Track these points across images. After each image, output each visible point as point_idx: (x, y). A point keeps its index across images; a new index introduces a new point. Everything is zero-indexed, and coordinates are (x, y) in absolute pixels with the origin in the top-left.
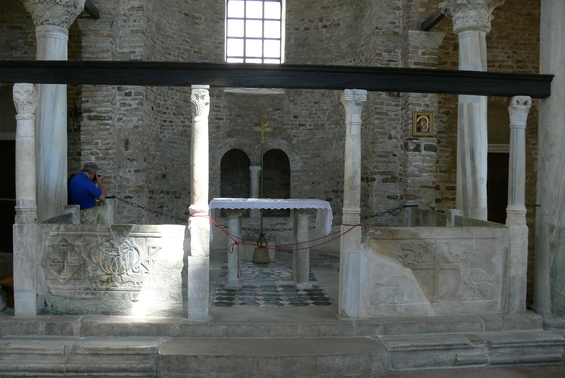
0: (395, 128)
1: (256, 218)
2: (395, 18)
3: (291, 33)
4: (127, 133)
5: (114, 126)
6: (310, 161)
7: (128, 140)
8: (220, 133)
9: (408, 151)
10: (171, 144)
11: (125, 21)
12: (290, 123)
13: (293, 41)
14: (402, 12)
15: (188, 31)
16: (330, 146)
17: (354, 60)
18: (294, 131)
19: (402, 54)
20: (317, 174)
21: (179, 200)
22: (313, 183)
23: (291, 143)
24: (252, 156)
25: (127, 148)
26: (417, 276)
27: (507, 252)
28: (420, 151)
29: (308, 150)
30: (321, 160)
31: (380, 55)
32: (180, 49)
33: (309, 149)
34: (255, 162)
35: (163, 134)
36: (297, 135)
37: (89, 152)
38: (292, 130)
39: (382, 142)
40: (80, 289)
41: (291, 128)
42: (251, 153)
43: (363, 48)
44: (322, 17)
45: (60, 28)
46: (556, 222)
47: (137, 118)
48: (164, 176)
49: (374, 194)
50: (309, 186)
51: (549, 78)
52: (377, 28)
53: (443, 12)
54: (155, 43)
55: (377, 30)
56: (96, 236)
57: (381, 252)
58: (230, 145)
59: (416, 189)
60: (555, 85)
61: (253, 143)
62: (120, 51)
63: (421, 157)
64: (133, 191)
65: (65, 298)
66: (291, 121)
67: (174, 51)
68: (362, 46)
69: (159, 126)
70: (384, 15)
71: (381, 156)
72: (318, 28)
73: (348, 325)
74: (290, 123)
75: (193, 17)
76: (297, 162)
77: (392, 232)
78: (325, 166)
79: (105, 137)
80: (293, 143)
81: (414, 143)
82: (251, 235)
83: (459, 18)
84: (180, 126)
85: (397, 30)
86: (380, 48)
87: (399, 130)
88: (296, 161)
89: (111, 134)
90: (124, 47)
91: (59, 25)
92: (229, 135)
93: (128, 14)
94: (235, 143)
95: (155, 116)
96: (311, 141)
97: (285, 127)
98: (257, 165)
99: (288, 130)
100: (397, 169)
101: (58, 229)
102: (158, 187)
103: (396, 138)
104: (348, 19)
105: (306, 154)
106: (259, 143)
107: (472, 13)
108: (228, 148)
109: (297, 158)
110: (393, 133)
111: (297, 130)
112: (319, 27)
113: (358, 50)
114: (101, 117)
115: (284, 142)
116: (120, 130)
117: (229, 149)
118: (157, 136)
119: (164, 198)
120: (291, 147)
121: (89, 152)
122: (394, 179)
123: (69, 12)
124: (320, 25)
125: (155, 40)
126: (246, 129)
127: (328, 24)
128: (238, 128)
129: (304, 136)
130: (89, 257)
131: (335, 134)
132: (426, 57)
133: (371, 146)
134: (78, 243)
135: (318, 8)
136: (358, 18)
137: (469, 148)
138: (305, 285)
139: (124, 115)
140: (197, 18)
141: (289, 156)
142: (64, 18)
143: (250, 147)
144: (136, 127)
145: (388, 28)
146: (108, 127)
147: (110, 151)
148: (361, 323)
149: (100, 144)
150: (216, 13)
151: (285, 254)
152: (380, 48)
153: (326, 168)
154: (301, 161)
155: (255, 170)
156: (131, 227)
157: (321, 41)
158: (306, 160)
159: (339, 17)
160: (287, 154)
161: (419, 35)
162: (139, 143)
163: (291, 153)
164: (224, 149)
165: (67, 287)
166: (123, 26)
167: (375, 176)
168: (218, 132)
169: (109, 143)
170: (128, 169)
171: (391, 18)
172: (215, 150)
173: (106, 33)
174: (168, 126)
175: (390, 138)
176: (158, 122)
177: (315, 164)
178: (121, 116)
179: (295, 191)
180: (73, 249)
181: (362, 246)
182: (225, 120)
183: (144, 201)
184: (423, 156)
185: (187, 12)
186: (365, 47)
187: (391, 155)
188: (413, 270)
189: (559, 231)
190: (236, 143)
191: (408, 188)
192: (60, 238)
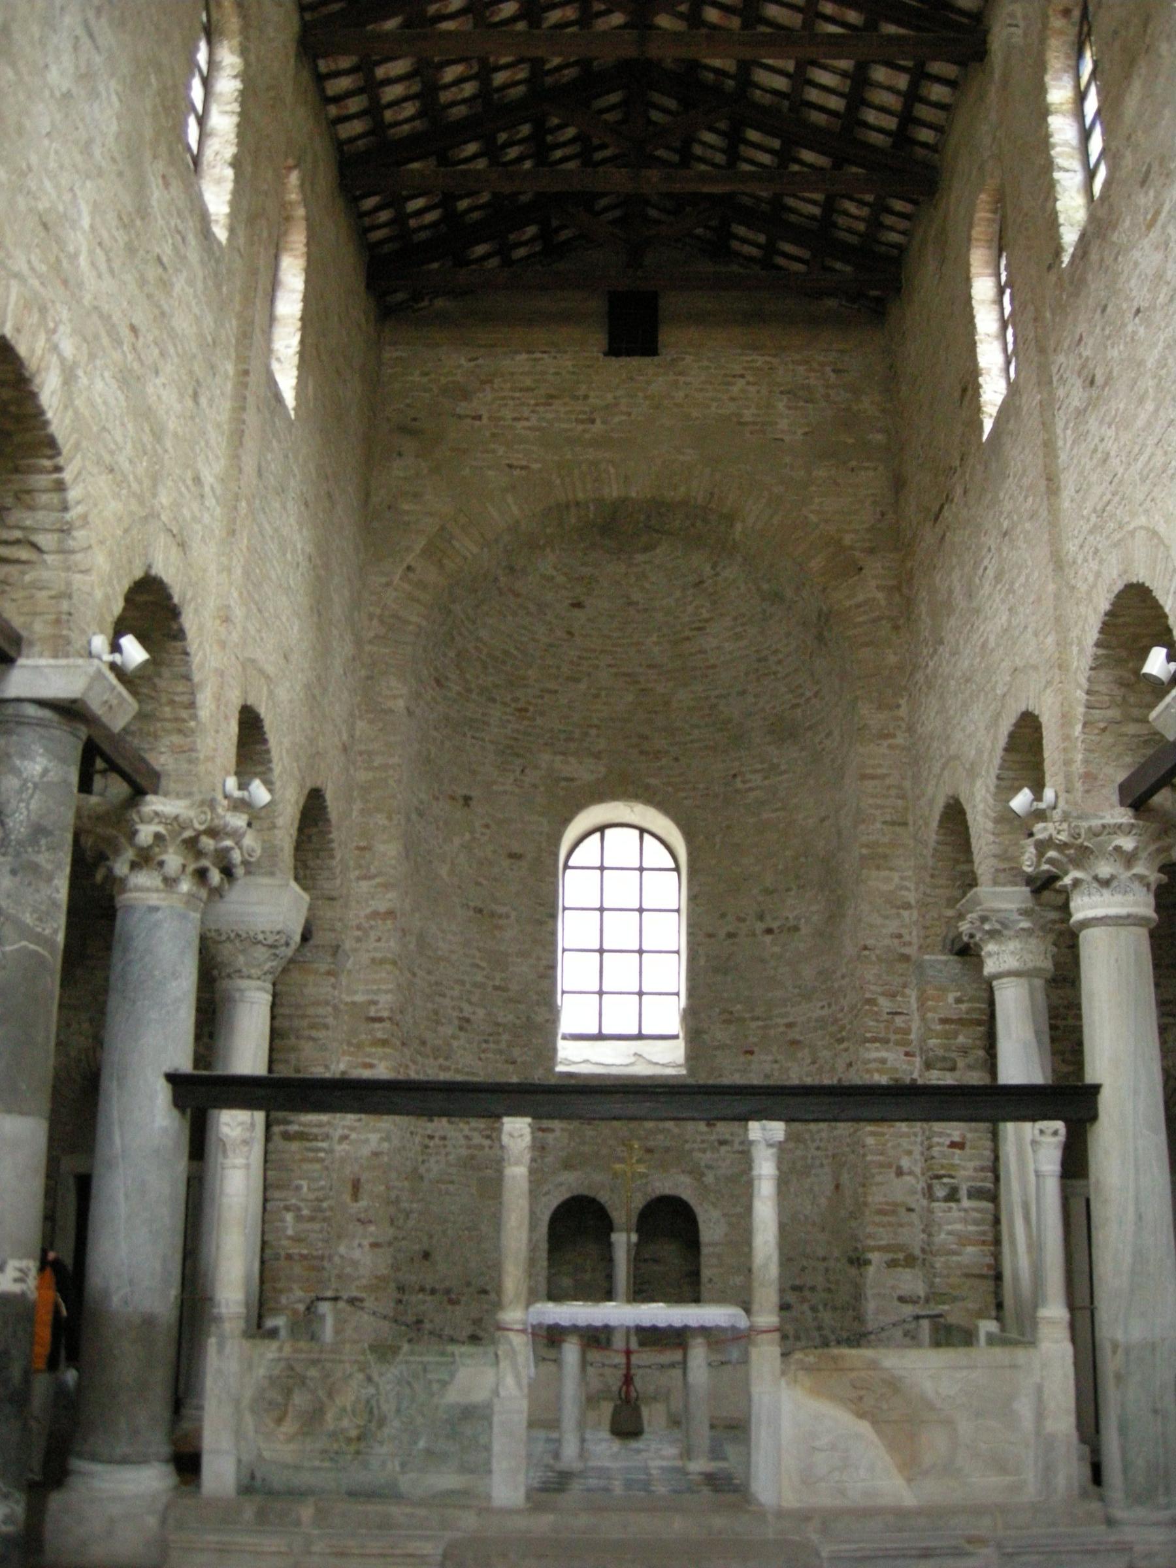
0: (909, 1153)
2: (902, 926)
3: (699, 945)
4: (356, 1168)
5: (330, 1151)
7: (359, 1180)
8: (546, 1160)
9: (934, 1201)
10: (443, 1187)
11: (359, 940)
12: (699, 1138)
13: (702, 962)
14: (915, 913)
15: (481, 944)
17: (830, 1005)
18: (709, 1155)
19: (918, 999)
21: (457, 1307)
25: (356, 1196)
26: (879, 1432)
27: (1039, 1389)
28: (958, 1201)
31: (871, 1002)
32: (463, 983)
35: (427, 1165)
37: (282, 1204)
39: (882, 1184)
40: (312, 1451)
43: (844, 982)
44: (763, 911)
45: (259, 983)
46: (1120, 1336)
47: (379, 1136)
48: (426, 1255)
49: (869, 1293)
50: (742, 1278)
51: (1096, 1089)
52: (865, 948)
53: (965, 939)
54: (414, 975)
55: (866, 953)
56: (341, 1362)
57: (816, 1392)
59: (952, 1280)
60: (1106, 1100)
62: (348, 999)
63: (962, 1214)
64: (365, 1287)
65: (286, 1466)
66: (701, 1133)
67: (452, 988)
68: (843, 977)
69: (419, 1148)
70: (879, 921)
71: (881, 1212)
72: (754, 935)
73: (761, 1515)
74: (699, 1138)
75: (492, 914)
77: (834, 1359)
79: (316, 1175)
81: (944, 1184)
83: (990, 954)
84: (461, 1147)
85: (906, 950)
86: (873, 988)
87: (918, 1157)
89: (327, 1168)
90: (355, 992)
91: (259, 978)
92: (568, 1165)
93: (366, 925)
95: (412, 1128)
97: (687, 1147)
100: (914, 1238)
101: (280, 1349)
102: (414, 1278)
103: (911, 1173)
104: (815, 918)
107: (1014, 945)
109: (715, 1214)
110: (905, 1163)
112: (757, 932)
113: (836, 985)
114: (307, 1134)
115: (686, 1179)
116: (343, 1161)
117: (567, 1196)
118: (415, 1170)
119: (424, 1302)
121: (282, 1204)
122: (910, 1261)
123: (275, 955)
124: (760, 926)
125: (416, 970)
126: (604, 1151)
127: (775, 925)
128: (586, 1149)
130: (330, 1395)
131: (794, 1163)
132: (964, 1007)
133: (860, 1190)
134: (313, 1372)
135: (755, 891)
136: (835, 914)
137: (1019, 1200)
138: (699, 1465)
139: (352, 1129)
140: (500, 916)
141: (698, 1210)
142: (267, 967)
144: (376, 1154)
145: (888, 946)
146: (322, 1155)
147: (325, 1205)
148: (781, 1514)
149: (305, 1189)
150: (540, 904)
152: (873, 988)
155: (622, 1241)
156: (399, 1348)
157: (763, 961)
159: (795, 913)
161: (946, 963)
162: (382, 1188)
165: (291, 1446)
166: (355, 950)
167: (870, 1256)
168: (542, 1157)
169: (322, 1188)
170: (356, 1242)
171: (892, 926)
173: (324, 968)
174: (437, 1146)
175: (900, 1173)
176: (418, 1139)
178: (346, 1132)
180: (304, 1383)
181: (783, 1383)
182: (558, 1133)
183: (387, 1307)
184: (965, 1210)
185: (479, 904)
186: (847, 980)
187: (902, 1211)
188: (875, 1423)
189: (1127, 1352)
191: (937, 1280)
192: (282, 1364)
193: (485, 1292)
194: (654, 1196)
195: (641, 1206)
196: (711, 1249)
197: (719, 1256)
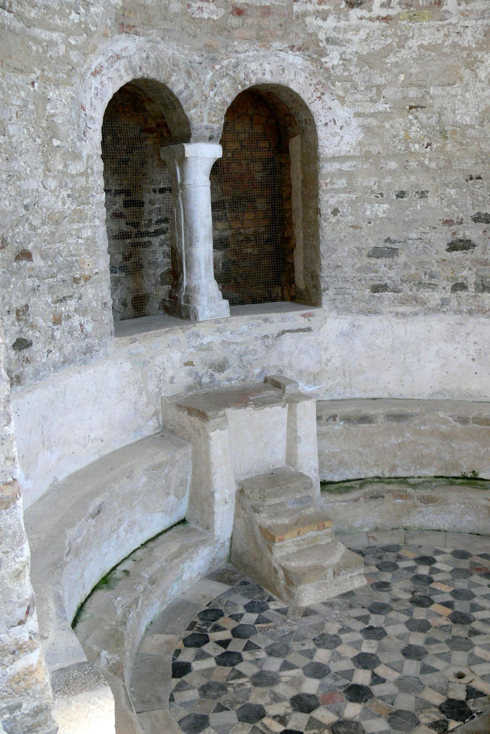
1: (217, 322)
6: (387, 125)
8: (92, 9)
16: (466, 73)
18: (331, 22)
20: (413, 164)
22: (401, 195)
23: (322, 64)
24: (195, 106)
29: (380, 88)
30: (429, 118)
33: (385, 86)
34: (207, 128)
36: (341, 36)
38: (324, 19)
41: (318, 14)
42: (191, 95)
50: (386, 206)
58: (130, 62)
61: (198, 59)
76: (341, 128)
78: (446, 138)
80: (329, 65)
82: (206, 380)
88: (339, 124)
94: (144, 55)
96: (392, 59)
98: (211, 139)
99: (309, 20)
105: (373, 101)
106: (214, 60)
108: (123, 72)
111: (339, 19)
117: (127, 79)
120: (320, 78)
129: (365, 40)
143: (189, 74)
151: (337, 427)
153: (449, 145)
154: (355, 122)
158: (373, 122)
160: (307, 102)
163: (320, 98)
164: (110, 79)
172: (82, 77)
177: (407, 130)
179: (338, 222)
190: (147, 57)
193: (26, 255)
194: (248, 84)
195: (229, 101)
196: (336, 166)
197: (350, 175)
